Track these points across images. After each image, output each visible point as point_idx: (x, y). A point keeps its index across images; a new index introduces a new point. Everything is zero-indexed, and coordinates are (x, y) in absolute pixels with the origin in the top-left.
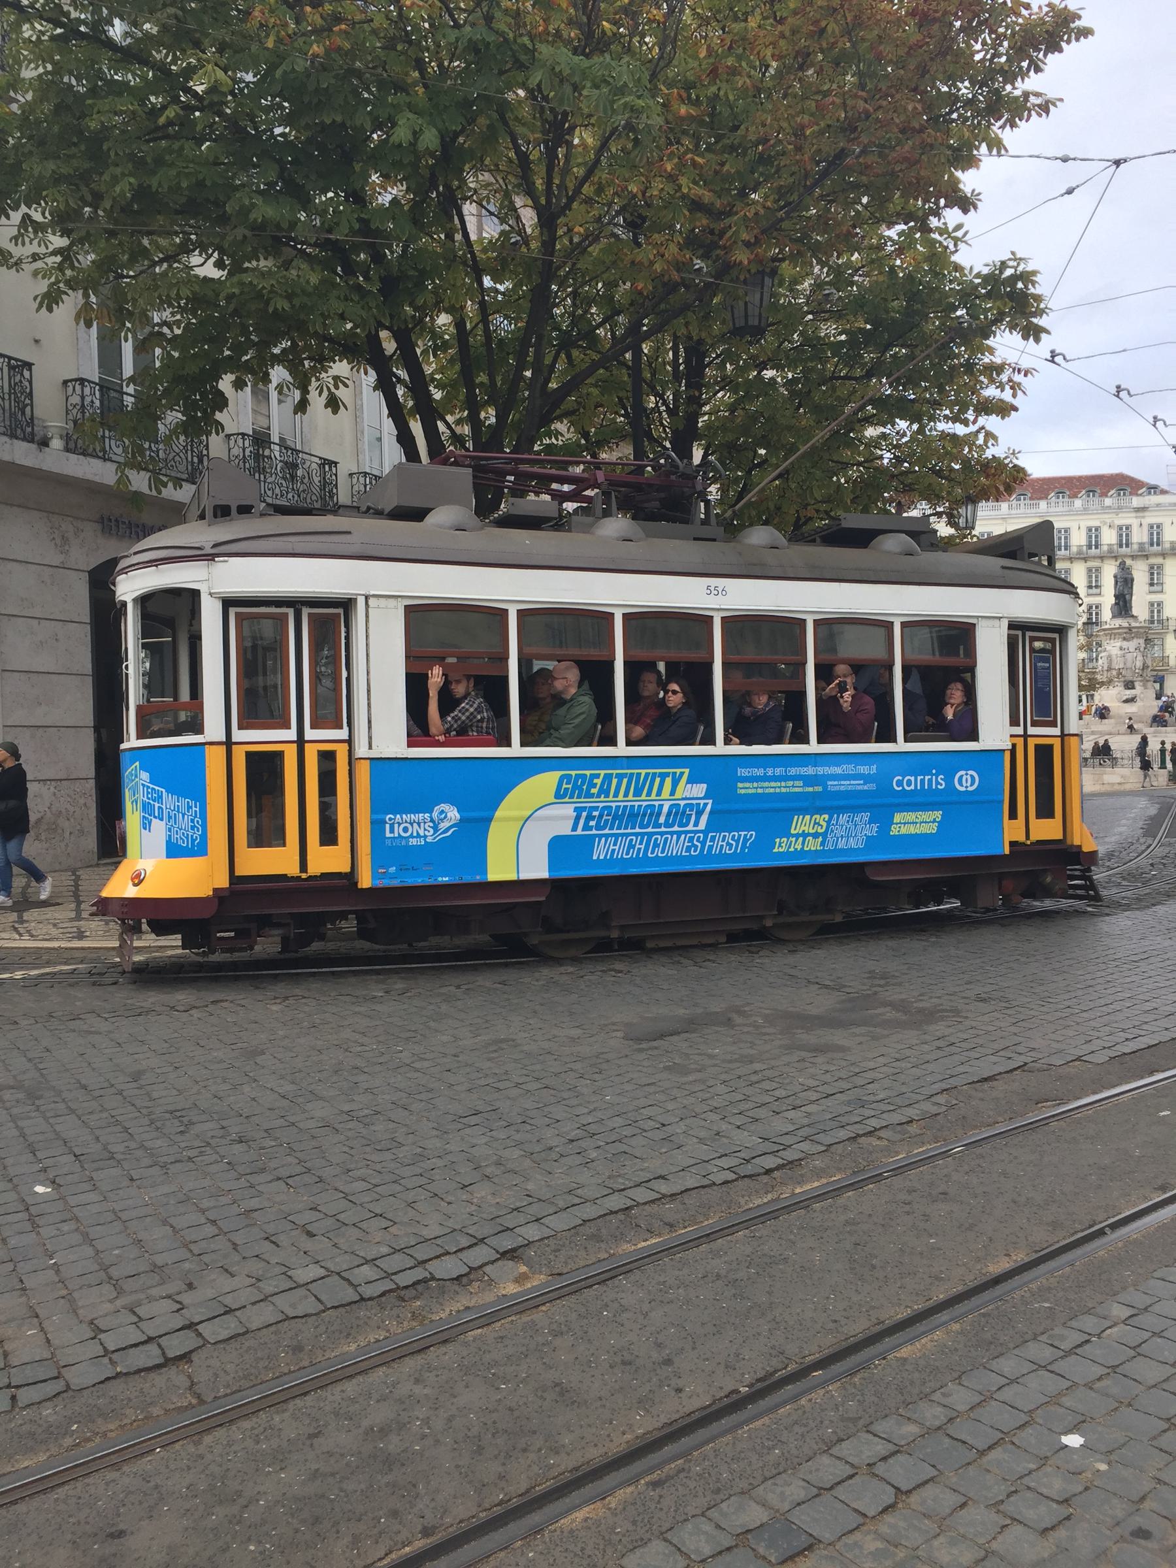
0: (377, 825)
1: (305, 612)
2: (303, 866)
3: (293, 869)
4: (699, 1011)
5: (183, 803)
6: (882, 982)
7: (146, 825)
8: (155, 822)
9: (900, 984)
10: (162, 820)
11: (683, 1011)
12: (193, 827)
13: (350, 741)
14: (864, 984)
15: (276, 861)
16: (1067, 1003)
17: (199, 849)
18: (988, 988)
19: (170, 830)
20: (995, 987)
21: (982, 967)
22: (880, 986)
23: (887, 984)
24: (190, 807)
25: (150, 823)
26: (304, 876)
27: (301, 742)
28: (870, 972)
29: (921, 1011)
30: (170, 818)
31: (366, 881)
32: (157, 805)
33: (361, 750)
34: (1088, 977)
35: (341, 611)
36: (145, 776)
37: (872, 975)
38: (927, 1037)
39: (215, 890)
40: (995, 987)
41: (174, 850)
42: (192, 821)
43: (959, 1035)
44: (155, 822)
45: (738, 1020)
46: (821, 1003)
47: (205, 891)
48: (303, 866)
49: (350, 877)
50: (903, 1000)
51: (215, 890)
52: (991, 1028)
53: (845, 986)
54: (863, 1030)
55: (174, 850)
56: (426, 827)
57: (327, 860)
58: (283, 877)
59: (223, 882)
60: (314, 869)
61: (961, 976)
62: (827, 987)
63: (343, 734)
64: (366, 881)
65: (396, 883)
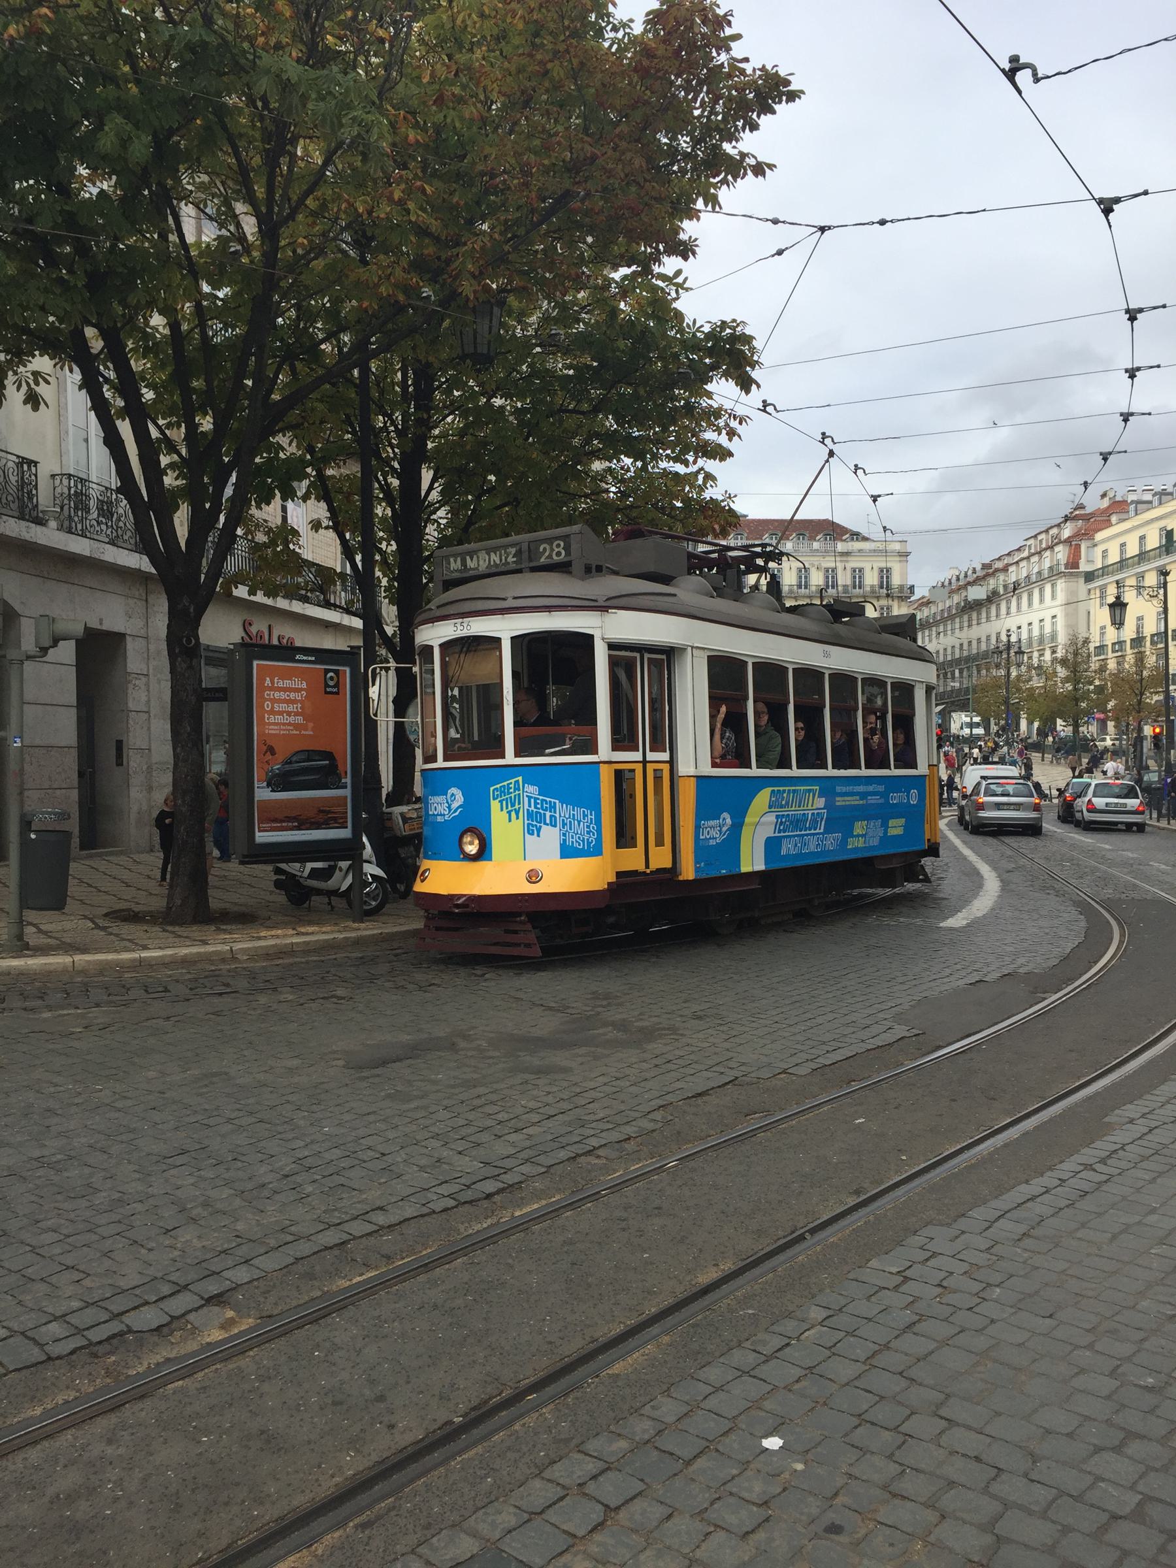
0: (697, 827)
1: (646, 656)
2: (647, 866)
3: (640, 866)
5: (578, 812)
6: (605, 1003)
7: (532, 829)
8: (545, 829)
10: (555, 826)
12: (588, 833)
13: (672, 762)
14: (586, 1005)
15: (632, 860)
16: (776, 1019)
17: (595, 850)
19: (564, 835)
20: (708, 1005)
21: (698, 986)
23: (609, 1004)
24: (585, 816)
25: (539, 830)
26: (648, 871)
27: (644, 762)
29: (641, 1030)
30: (564, 824)
31: (688, 872)
32: (548, 814)
33: (686, 768)
35: (664, 657)
36: (532, 790)
39: (609, 884)
40: (708, 1005)
41: (567, 852)
42: (588, 827)
43: (677, 1052)
44: (545, 829)
45: (462, 1044)
46: (546, 1025)
47: (599, 885)
48: (647, 866)
49: (674, 869)
51: (609, 884)
54: (583, 1050)
55: (567, 852)
56: (716, 830)
57: (661, 859)
58: (635, 873)
59: (612, 878)
60: (654, 865)
62: (550, 1009)
63: (665, 756)
64: (688, 872)
65: (704, 876)
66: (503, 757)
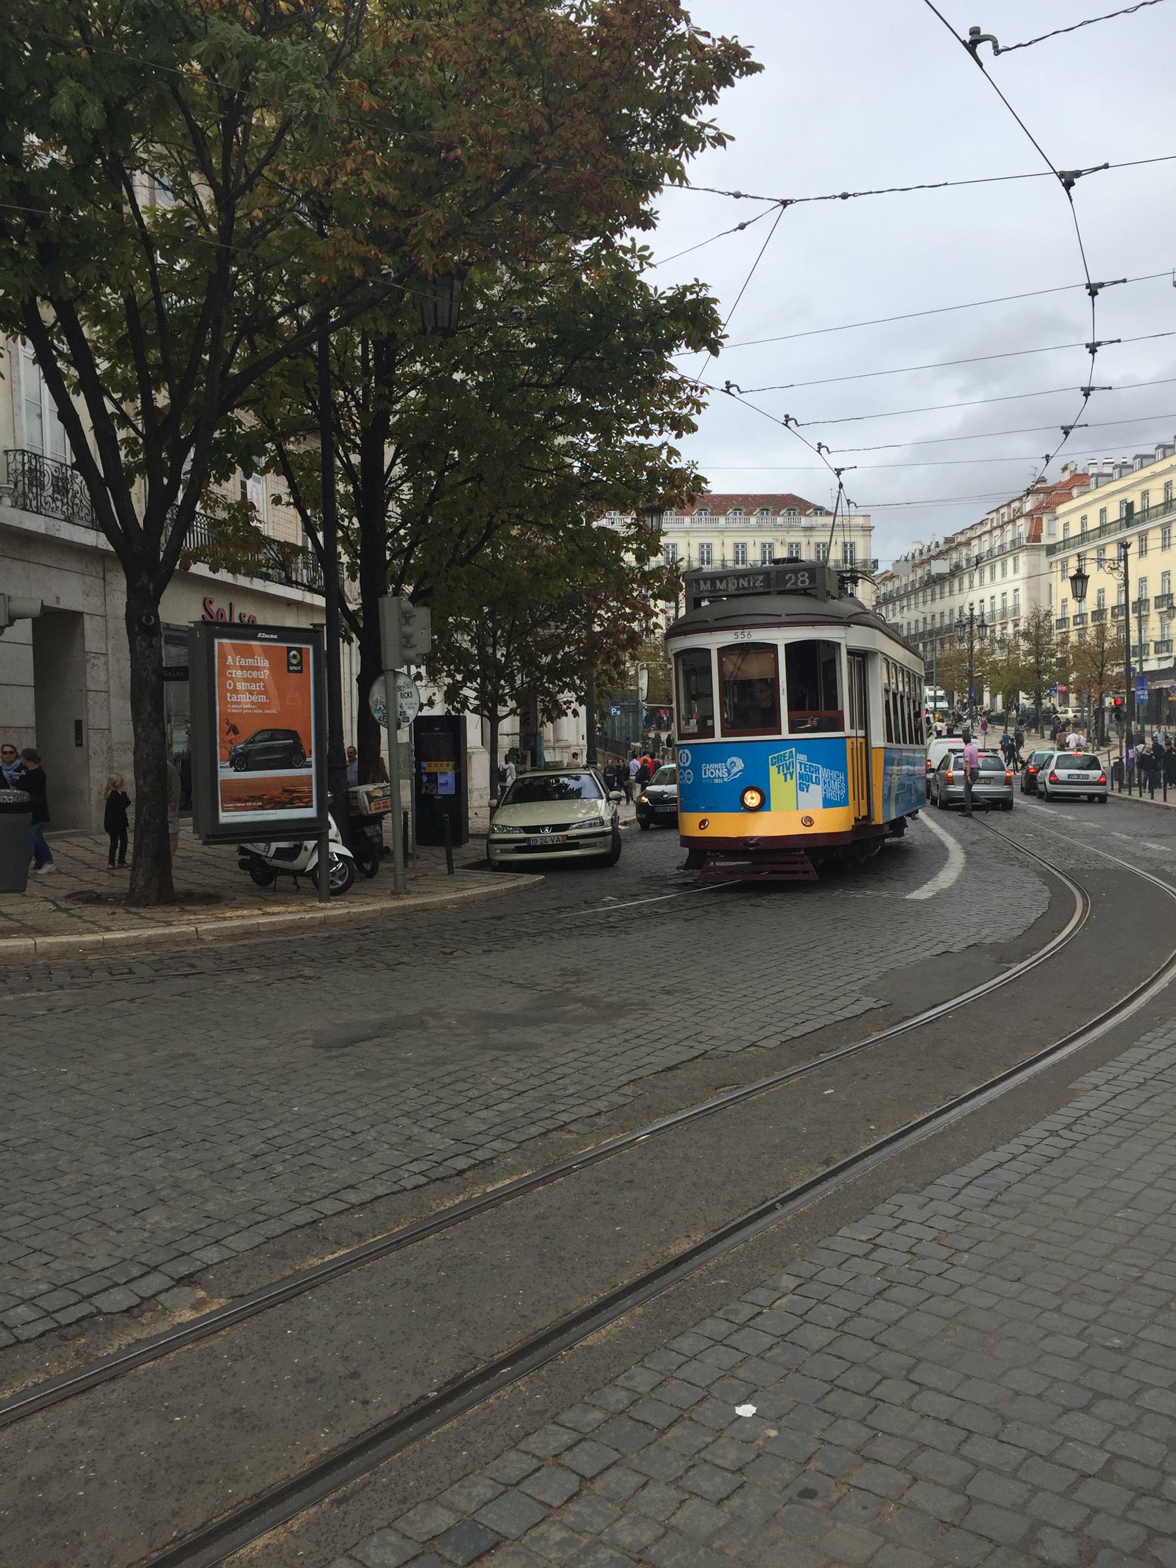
4: (391, 1014)
6: (574, 979)
9: (591, 980)
11: (377, 1016)
14: (556, 982)
16: (745, 993)
18: (673, 981)
20: (678, 980)
21: (667, 961)
22: (572, 983)
23: (579, 981)
28: (561, 970)
29: (610, 1005)
34: (764, 966)
37: (564, 972)
38: (617, 1031)
40: (678, 980)
43: (647, 1027)
45: (432, 1022)
46: (514, 1001)
50: (593, 996)
52: (675, 1019)
53: (538, 984)
54: (554, 1026)
61: (649, 970)
62: (520, 986)
66: (780, 733)
